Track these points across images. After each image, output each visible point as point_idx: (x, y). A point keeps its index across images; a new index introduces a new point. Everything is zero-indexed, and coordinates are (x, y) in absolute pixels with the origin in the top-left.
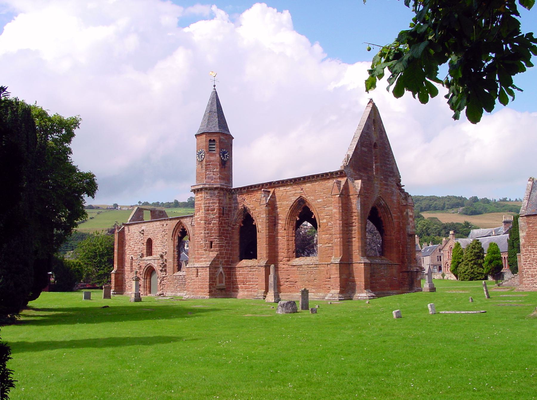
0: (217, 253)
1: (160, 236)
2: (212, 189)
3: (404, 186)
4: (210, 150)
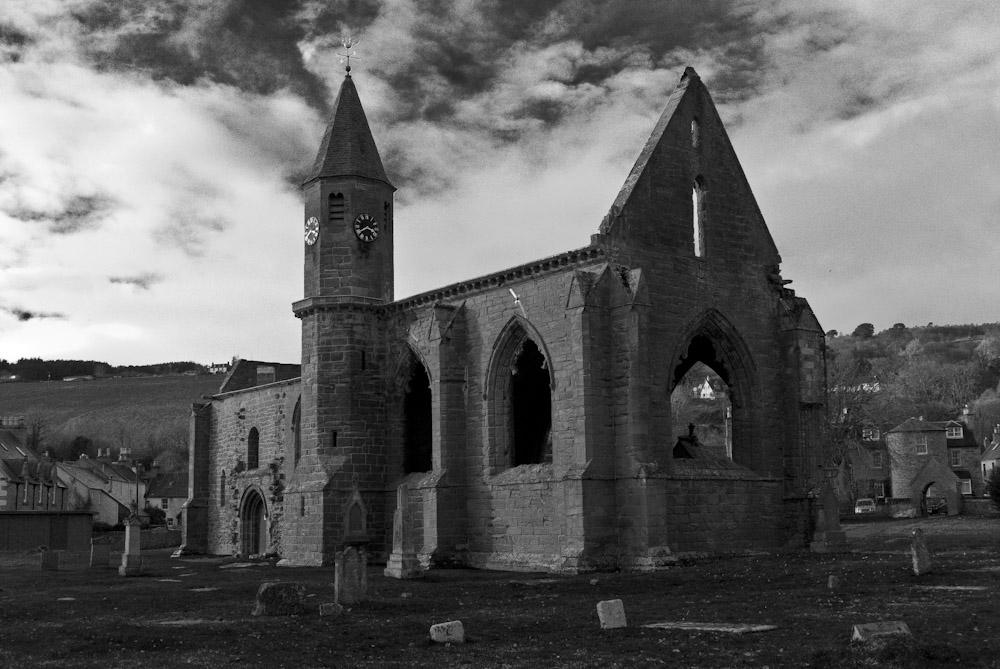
0: (344, 458)
1: (271, 422)
2: (335, 308)
3: (790, 282)
4: (332, 219)
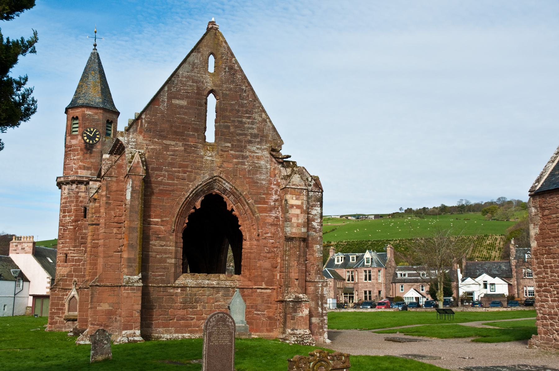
3: (288, 157)
